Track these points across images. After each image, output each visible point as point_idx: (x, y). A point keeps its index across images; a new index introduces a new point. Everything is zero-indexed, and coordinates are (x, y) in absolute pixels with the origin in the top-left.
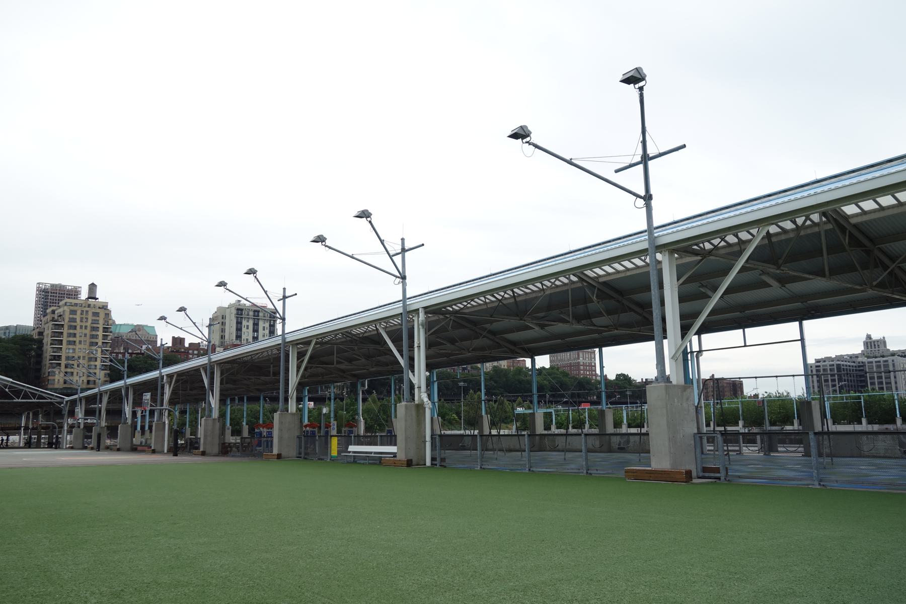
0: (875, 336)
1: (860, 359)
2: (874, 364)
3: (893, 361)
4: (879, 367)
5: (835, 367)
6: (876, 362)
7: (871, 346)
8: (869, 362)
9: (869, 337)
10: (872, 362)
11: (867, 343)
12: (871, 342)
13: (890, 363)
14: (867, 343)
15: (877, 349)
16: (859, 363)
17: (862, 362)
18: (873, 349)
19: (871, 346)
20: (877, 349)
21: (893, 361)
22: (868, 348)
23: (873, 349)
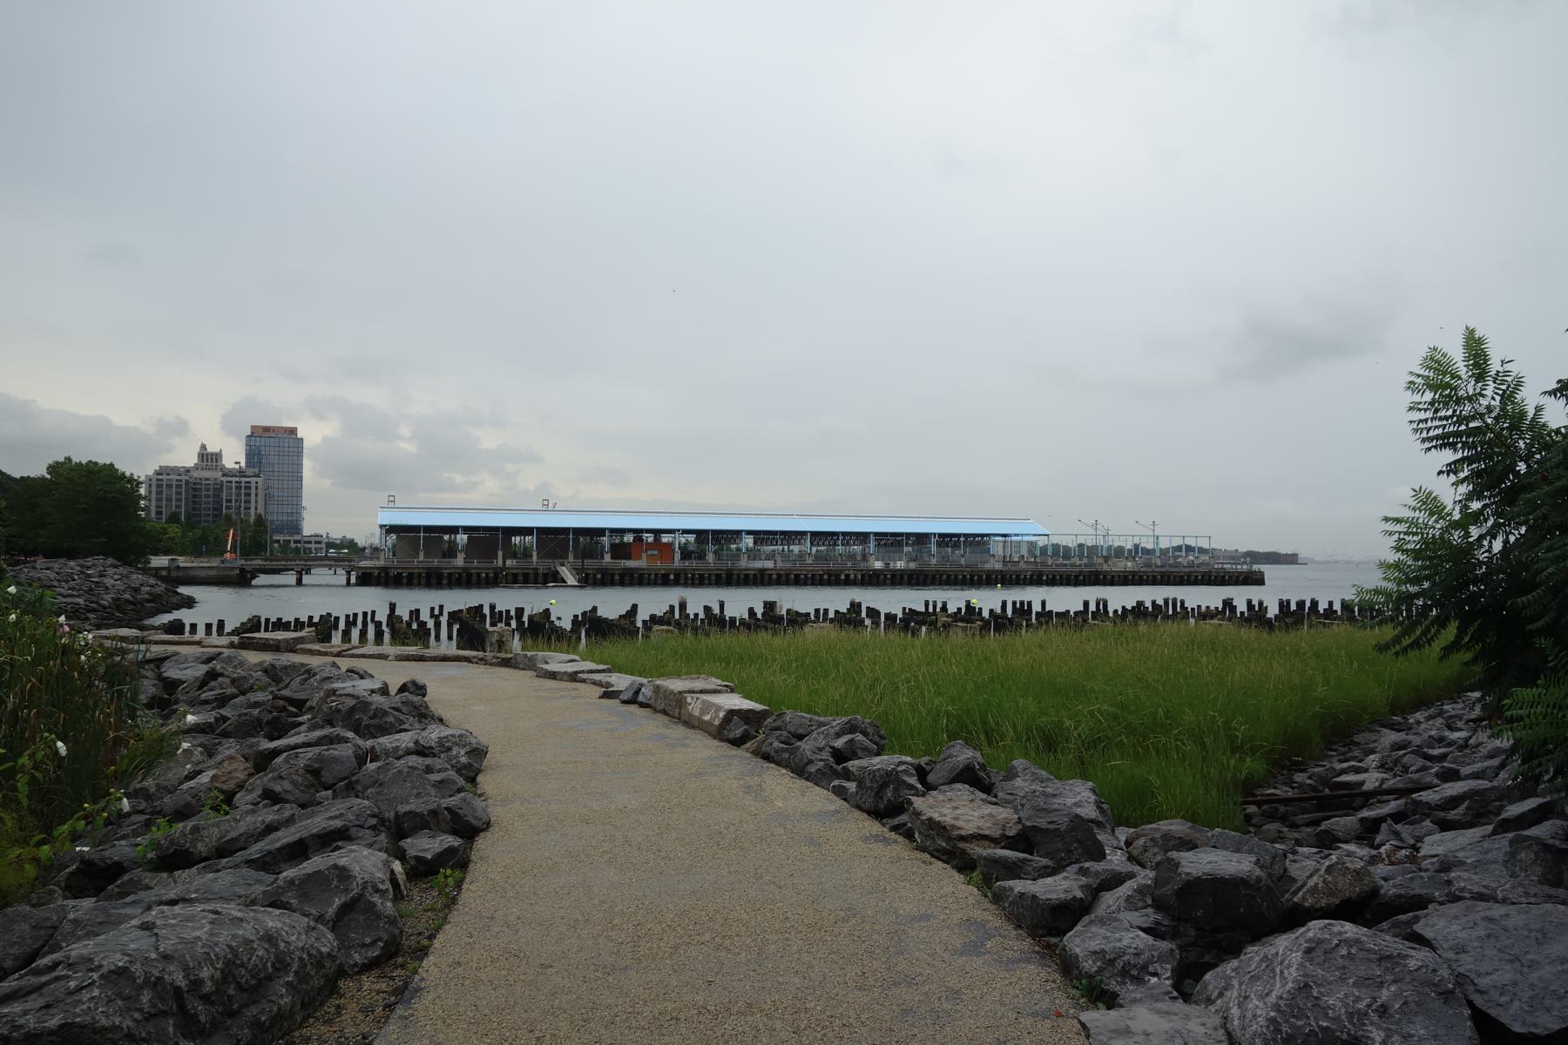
0: (210, 450)
1: (196, 474)
2: (234, 485)
3: (257, 483)
4: (239, 488)
5: (183, 483)
6: (236, 482)
7: (207, 459)
8: (227, 482)
9: (203, 447)
10: (231, 482)
11: (203, 455)
12: (207, 455)
13: (253, 485)
14: (203, 455)
15: (214, 464)
16: (196, 479)
17: (201, 479)
18: (209, 463)
19: (207, 459)
20: (214, 464)
21: (257, 483)
22: (203, 461)
23: (209, 463)
